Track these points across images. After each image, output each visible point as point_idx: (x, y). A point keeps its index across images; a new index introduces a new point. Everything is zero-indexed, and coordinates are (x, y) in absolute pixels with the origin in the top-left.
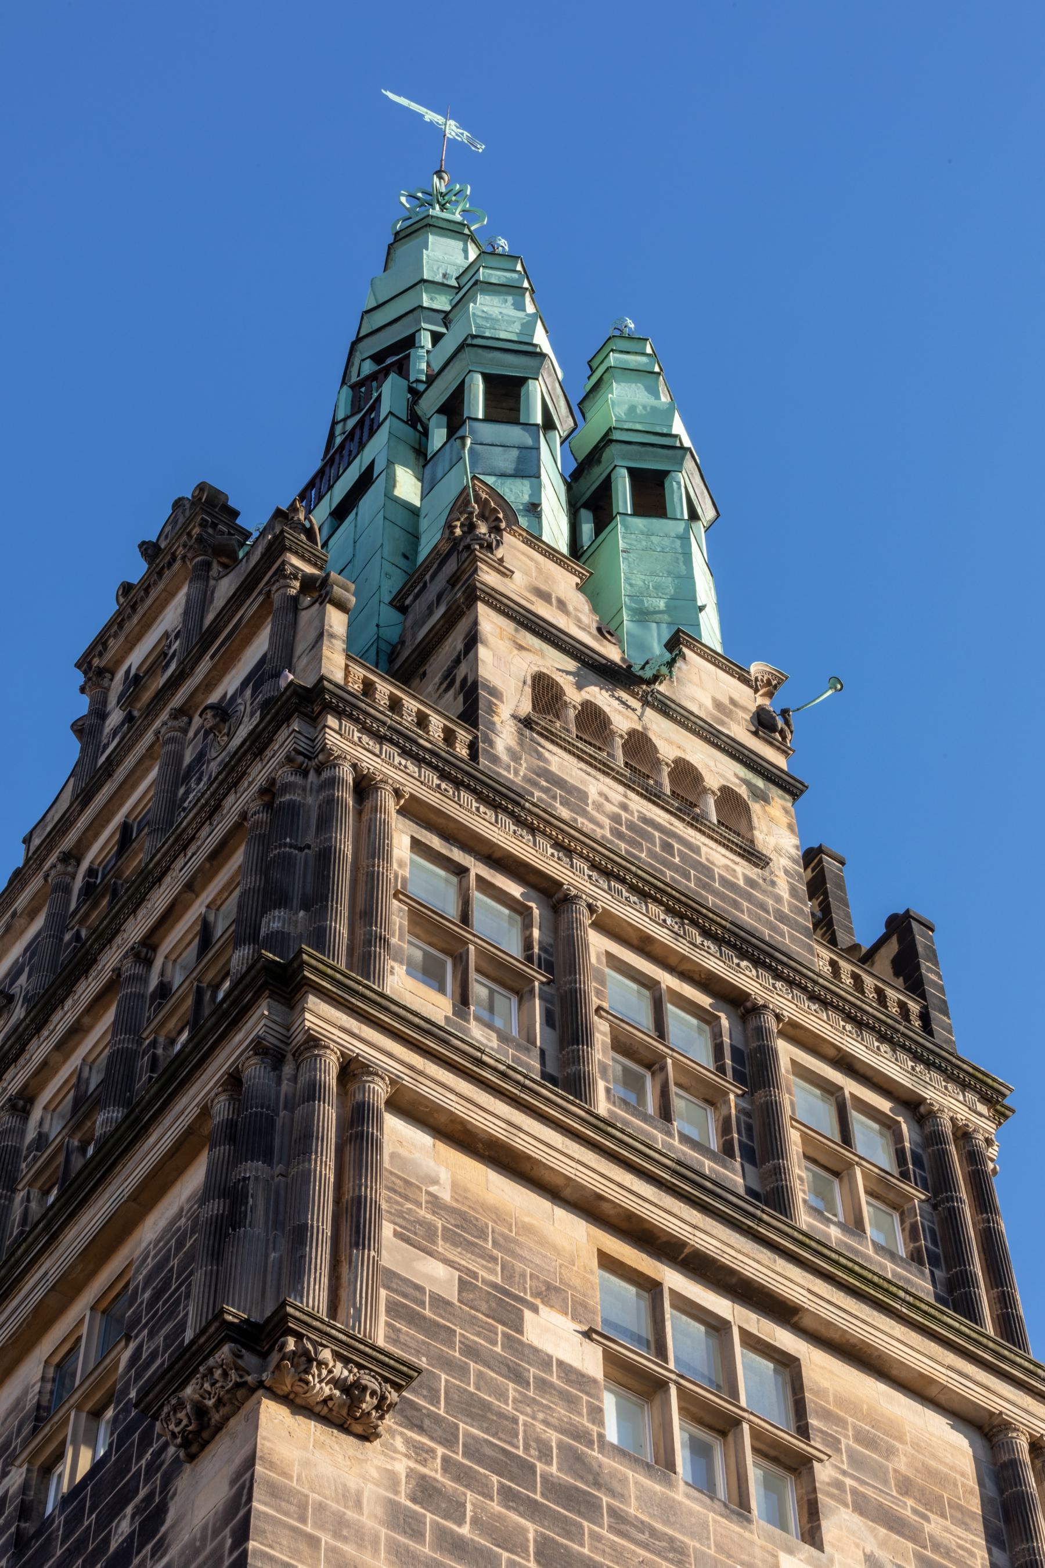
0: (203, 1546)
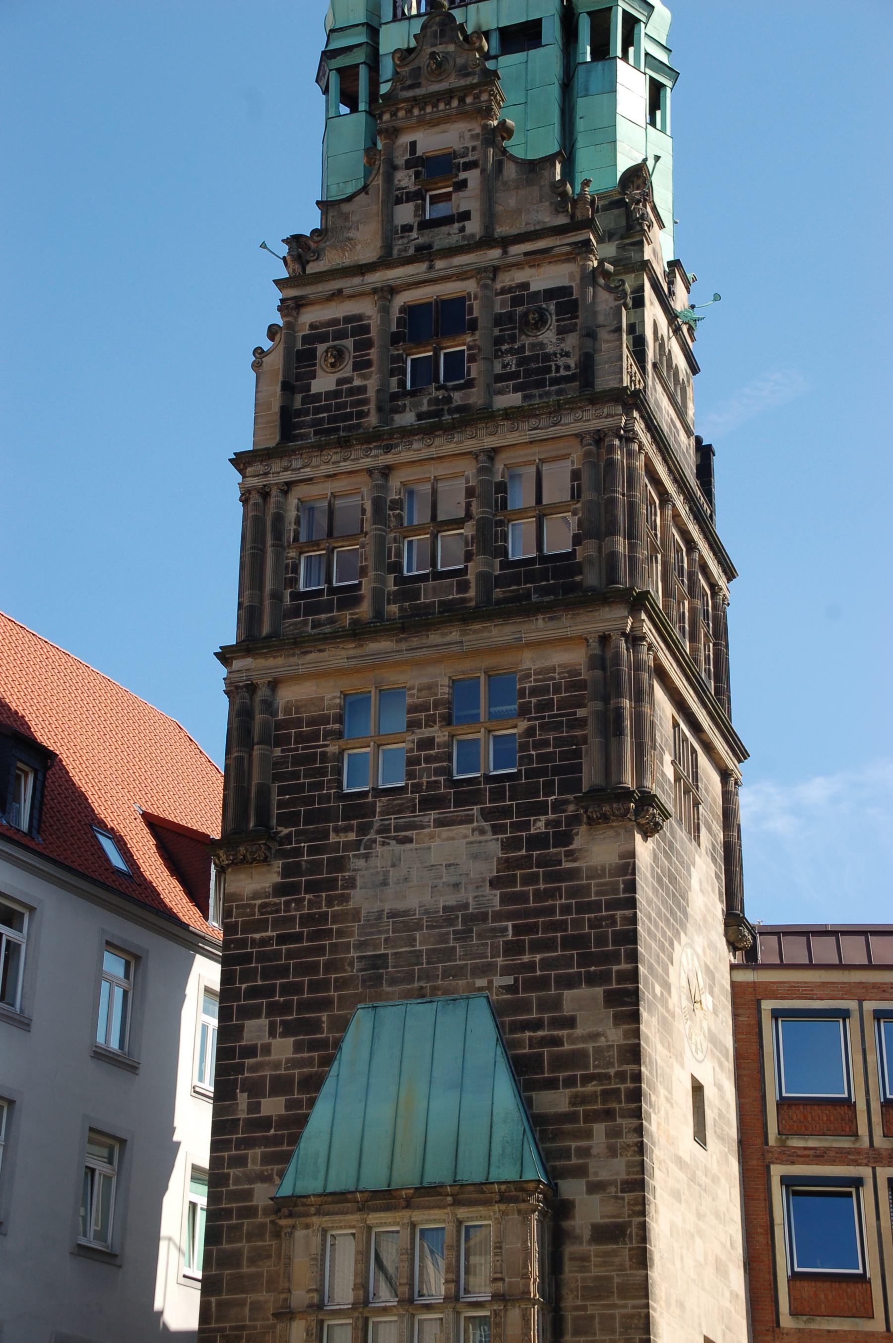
0: (602, 875)
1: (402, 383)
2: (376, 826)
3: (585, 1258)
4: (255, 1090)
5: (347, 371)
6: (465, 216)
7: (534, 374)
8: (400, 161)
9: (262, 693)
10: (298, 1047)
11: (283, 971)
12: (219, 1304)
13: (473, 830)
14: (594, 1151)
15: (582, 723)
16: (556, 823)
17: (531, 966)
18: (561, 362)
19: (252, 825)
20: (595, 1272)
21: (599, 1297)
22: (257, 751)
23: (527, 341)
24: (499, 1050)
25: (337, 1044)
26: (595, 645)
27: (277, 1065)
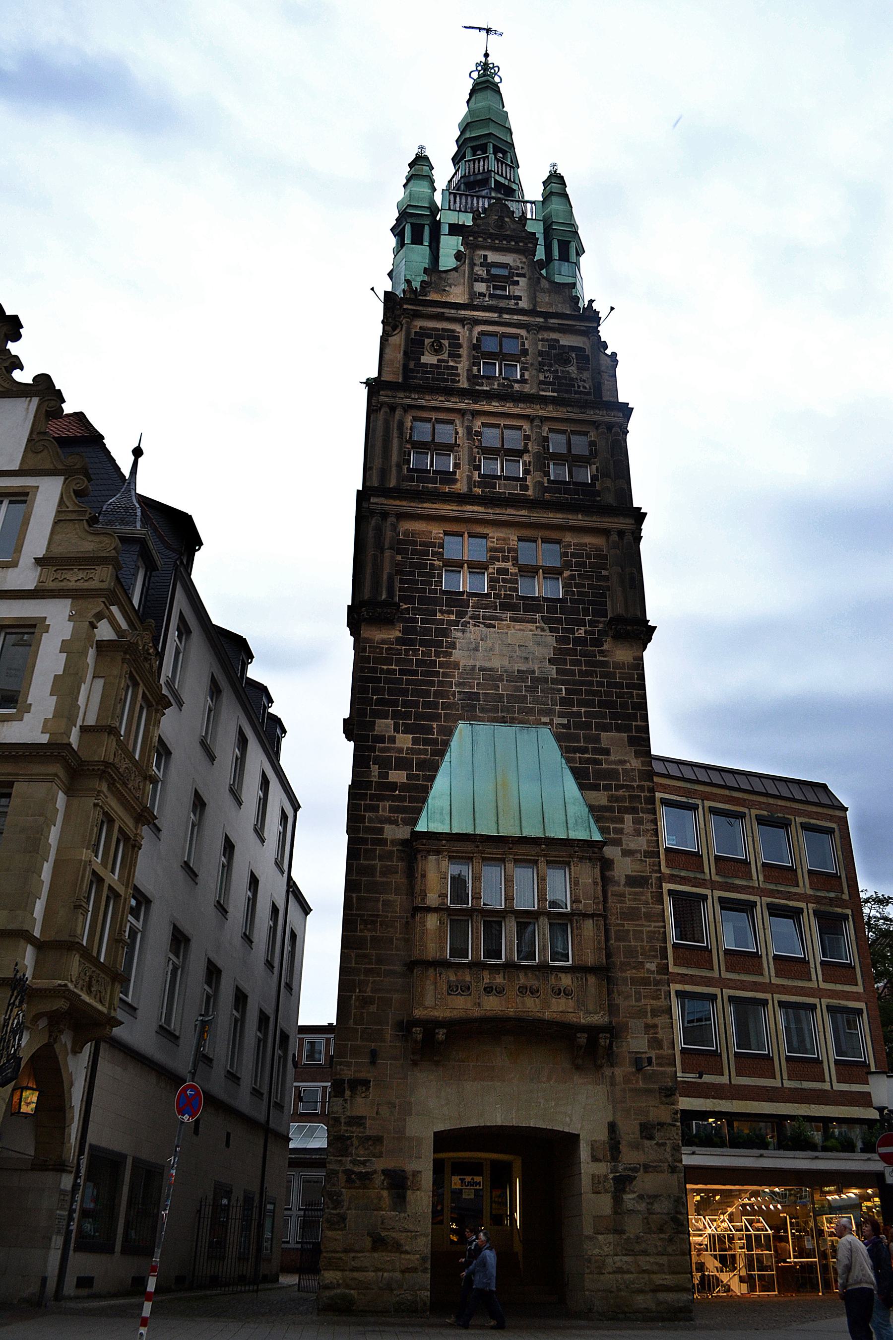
1: (479, 370)
2: (469, 614)
3: (622, 895)
4: (385, 764)
5: (445, 356)
6: (519, 298)
7: (564, 384)
8: (478, 263)
9: (391, 519)
10: (415, 741)
11: (405, 692)
12: (358, 898)
13: (537, 627)
14: (625, 831)
15: (606, 579)
16: (592, 633)
17: (579, 714)
18: (581, 384)
19: (384, 597)
20: (628, 904)
21: (633, 920)
22: (387, 553)
23: (560, 368)
24: (564, 761)
25: (446, 744)
26: (614, 537)
27: (400, 750)
